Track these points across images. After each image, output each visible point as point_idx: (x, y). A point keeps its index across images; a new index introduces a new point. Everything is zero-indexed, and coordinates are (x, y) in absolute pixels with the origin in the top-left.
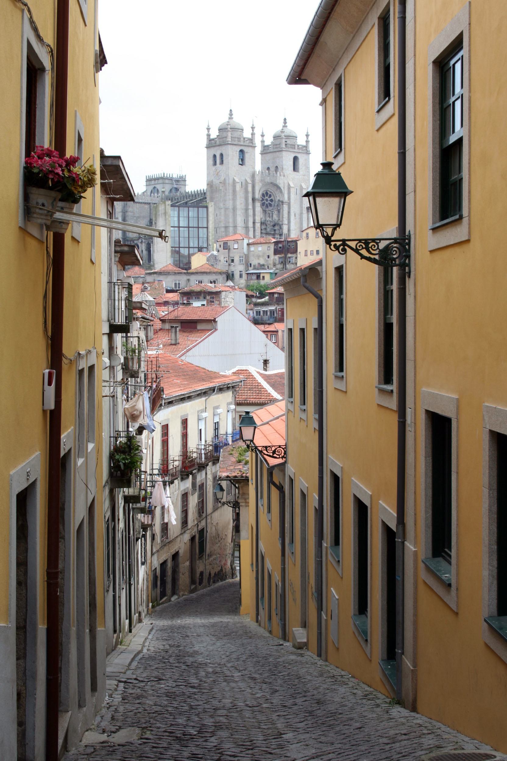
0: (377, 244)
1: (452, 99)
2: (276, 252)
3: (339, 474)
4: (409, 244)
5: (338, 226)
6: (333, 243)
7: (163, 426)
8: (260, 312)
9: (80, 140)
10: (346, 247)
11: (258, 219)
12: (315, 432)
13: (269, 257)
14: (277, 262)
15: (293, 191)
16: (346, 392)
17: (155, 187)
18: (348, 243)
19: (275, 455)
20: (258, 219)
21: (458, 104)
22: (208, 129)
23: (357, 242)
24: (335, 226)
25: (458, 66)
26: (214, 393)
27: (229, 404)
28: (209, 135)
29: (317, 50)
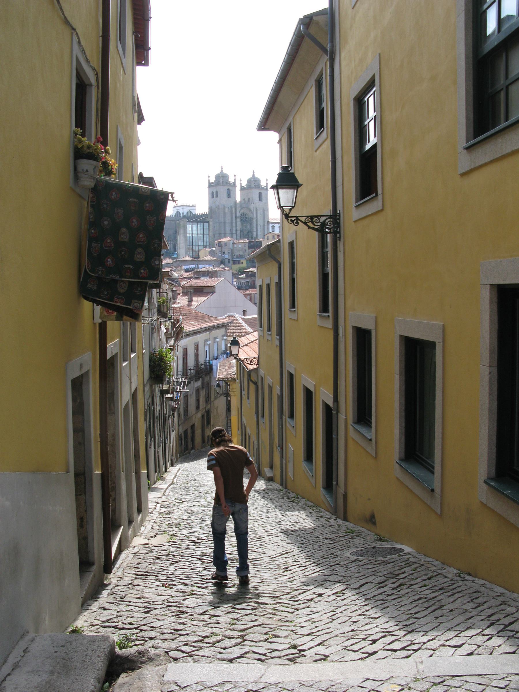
0: (319, 219)
1: (368, 121)
2: (250, 248)
3: (293, 373)
4: (339, 219)
5: (293, 207)
6: (290, 219)
7: (184, 349)
9: (121, 148)
11: (238, 229)
15: (259, 212)
16: (297, 320)
17: (178, 211)
18: (299, 218)
19: (252, 363)
20: (238, 229)
21: (372, 124)
23: (306, 218)
24: (290, 208)
25: (371, 100)
27: (223, 336)
28: (209, 180)
29: (276, 108)
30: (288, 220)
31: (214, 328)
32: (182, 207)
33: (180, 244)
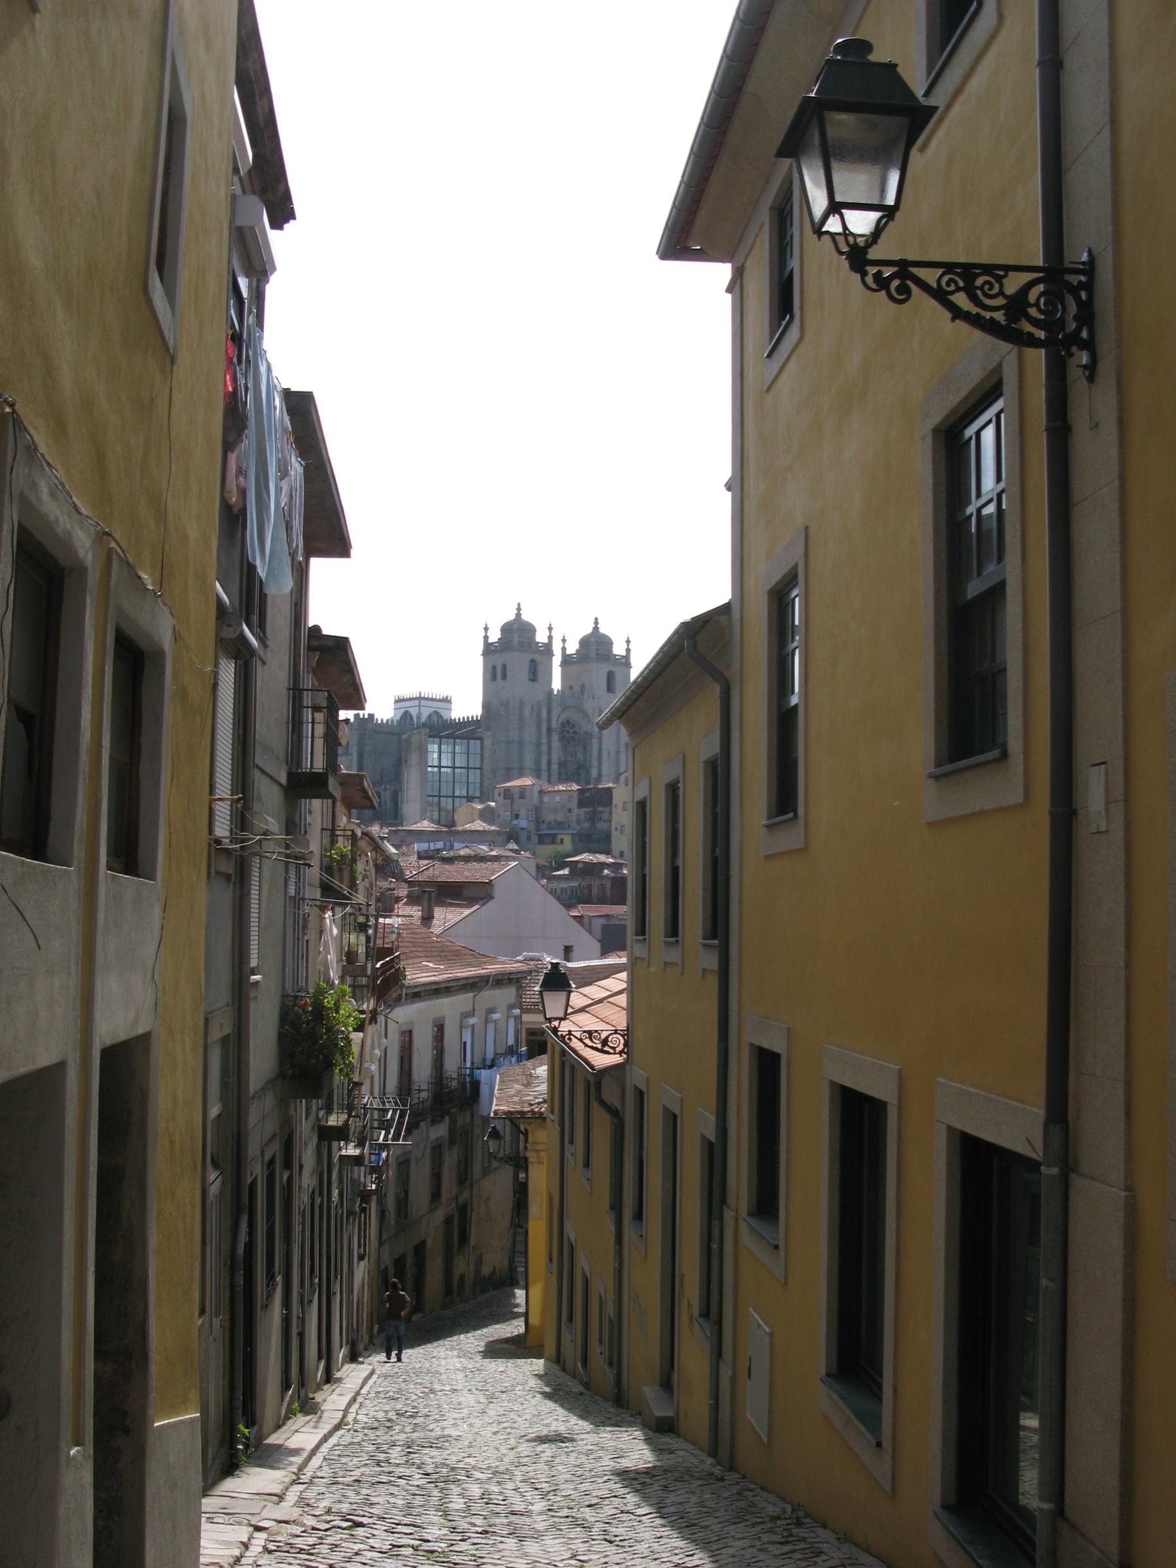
0: (999, 280)
6: (871, 270)
7: (403, 1033)
8: (556, 890)
10: (908, 282)
12: (703, 977)
13: (570, 811)
14: (582, 819)
17: (406, 712)
18: (915, 270)
19: (606, 1048)
22: (486, 629)
23: (940, 272)
26: (488, 986)
27: (511, 1007)
28: (486, 638)
30: (864, 274)
31: (487, 982)
32: (416, 703)
33: (408, 790)
